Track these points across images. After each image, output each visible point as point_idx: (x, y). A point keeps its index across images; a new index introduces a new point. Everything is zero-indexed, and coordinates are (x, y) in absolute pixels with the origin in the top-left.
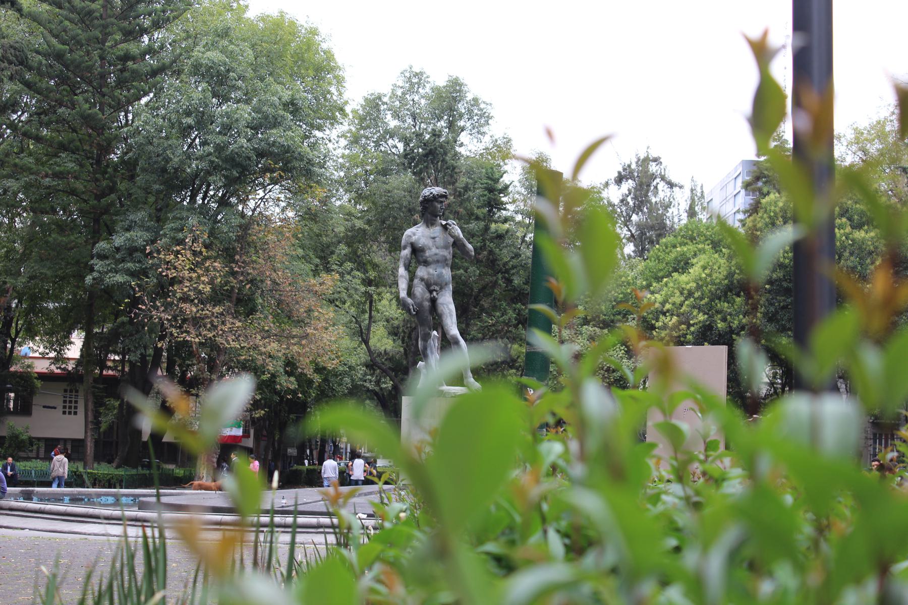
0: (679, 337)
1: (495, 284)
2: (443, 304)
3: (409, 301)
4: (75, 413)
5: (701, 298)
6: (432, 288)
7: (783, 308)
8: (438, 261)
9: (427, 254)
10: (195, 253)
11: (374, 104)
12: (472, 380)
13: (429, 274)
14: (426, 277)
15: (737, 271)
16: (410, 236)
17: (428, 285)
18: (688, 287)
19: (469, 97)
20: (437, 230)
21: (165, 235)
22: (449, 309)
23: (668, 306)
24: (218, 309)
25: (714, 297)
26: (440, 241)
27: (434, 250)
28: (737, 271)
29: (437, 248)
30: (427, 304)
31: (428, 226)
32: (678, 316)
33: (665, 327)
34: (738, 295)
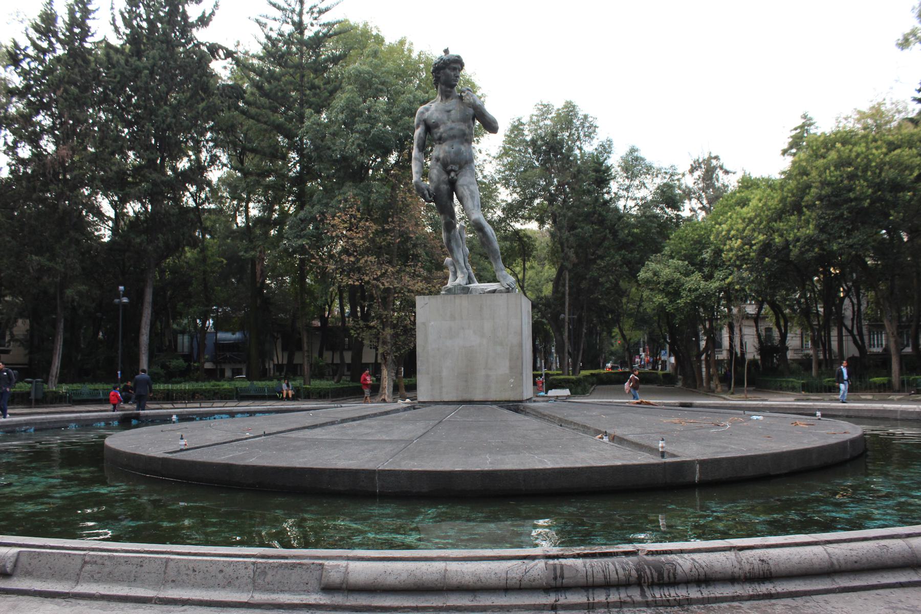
0: (744, 255)
1: (605, 238)
2: (462, 186)
5: (761, 223)
6: (449, 168)
7: (833, 220)
8: (453, 137)
9: (441, 130)
14: (441, 156)
20: (452, 103)
22: (472, 192)
23: (733, 233)
25: (771, 220)
26: (455, 114)
27: (449, 124)
29: (453, 122)
30: (444, 187)
32: (742, 239)
33: (731, 249)
34: (792, 214)
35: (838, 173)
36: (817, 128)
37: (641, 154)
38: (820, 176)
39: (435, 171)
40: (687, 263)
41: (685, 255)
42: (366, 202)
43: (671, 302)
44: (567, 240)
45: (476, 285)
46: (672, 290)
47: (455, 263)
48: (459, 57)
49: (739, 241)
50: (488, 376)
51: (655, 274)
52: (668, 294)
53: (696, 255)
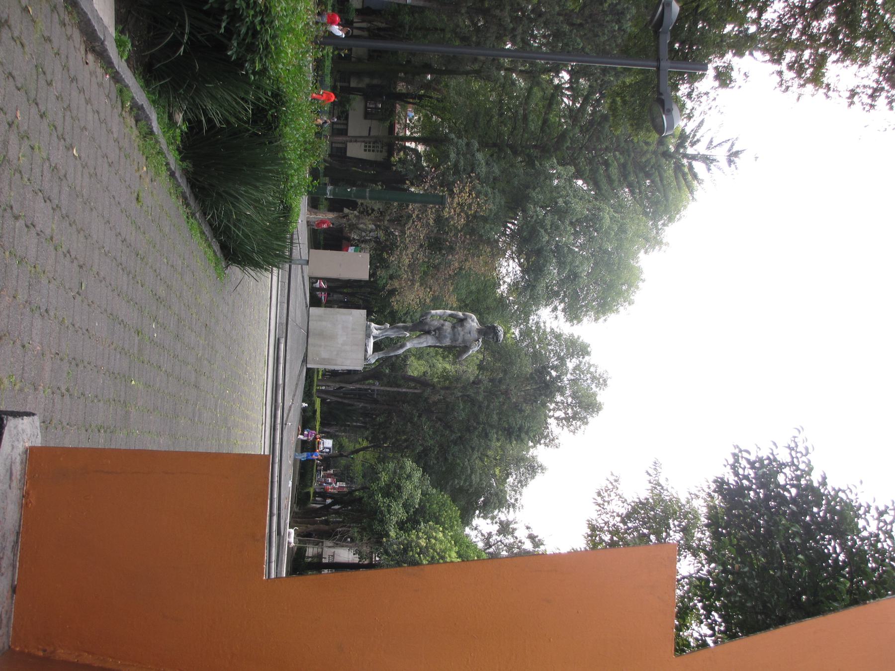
4: (365, 150)
8: (454, 335)
10: (470, 205)
11: (582, 350)
17: (439, 329)
20: (475, 335)
21: (483, 187)
23: (433, 541)
24: (431, 222)
26: (468, 337)
27: (462, 333)
30: (427, 328)
32: (426, 547)
33: (418, 537)
37: (539, 477)
40: (417, 506)
41: (424, 506)
42: (485, 219)
43: (381, 489)
44: (452, 394)
45: (372, 341)
46: (392, 490)
47: (386, 330)
50: (321, 346)
51: (409, 477)
52: (388, 486)
53: (424, 517)
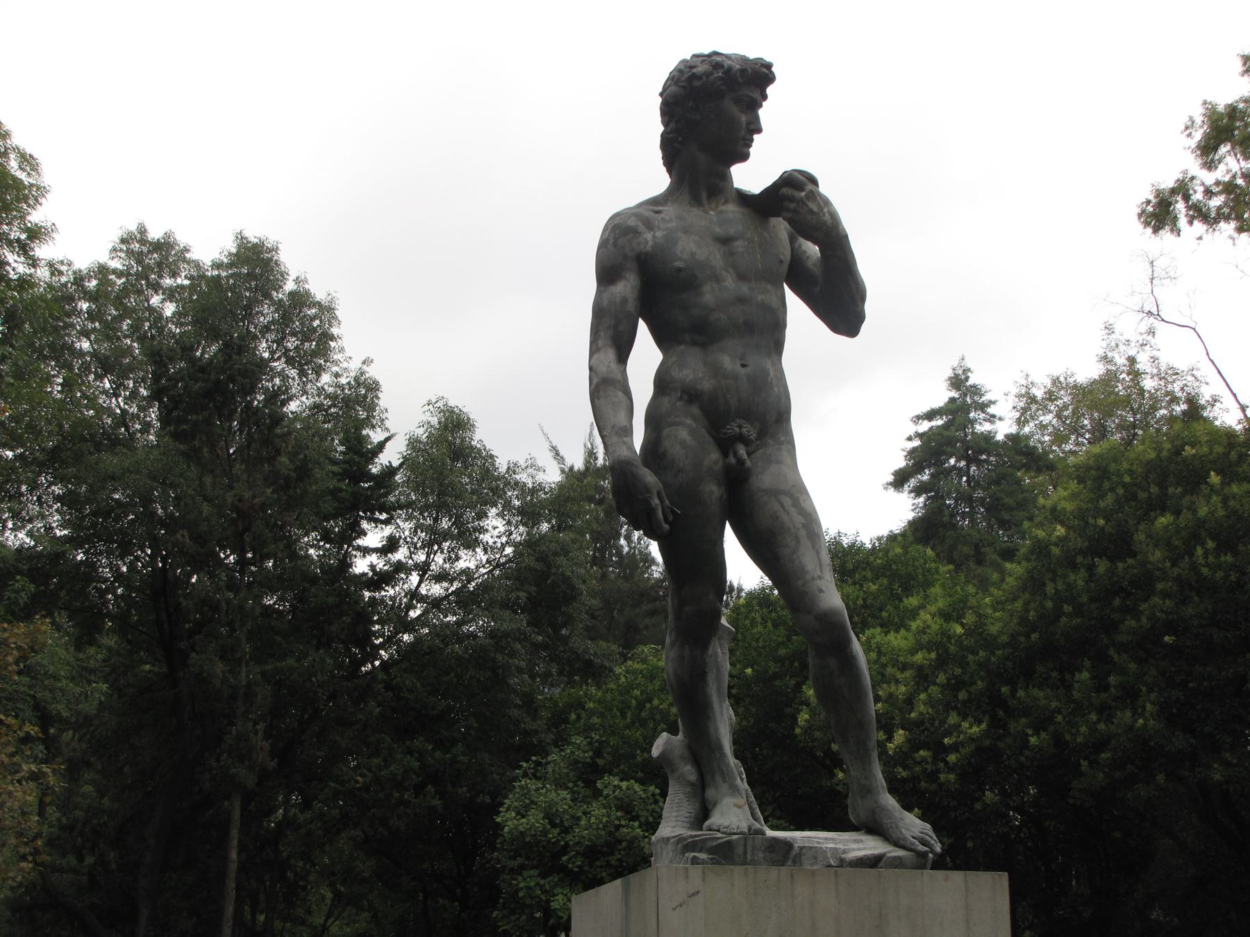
2: (775, 493)
3: (649, 477)
6: (733, 428)
9: (709, 295)
12: (890, 802)
13: (716, 371)
14: (707, 385)
15: (1067, 608)
16: (635, 232)
18: (919, 657)
19: (290, 286)
28: (1067, 608)
29: (742, 277)
30: (713, 491)
31: (696, 201)
35: (1229, 558)
36: (992, 418)
38: (1173, 565)
39: (684, 434)
47: (701, 750)
48: (769, 66)
49: (900, 736)
